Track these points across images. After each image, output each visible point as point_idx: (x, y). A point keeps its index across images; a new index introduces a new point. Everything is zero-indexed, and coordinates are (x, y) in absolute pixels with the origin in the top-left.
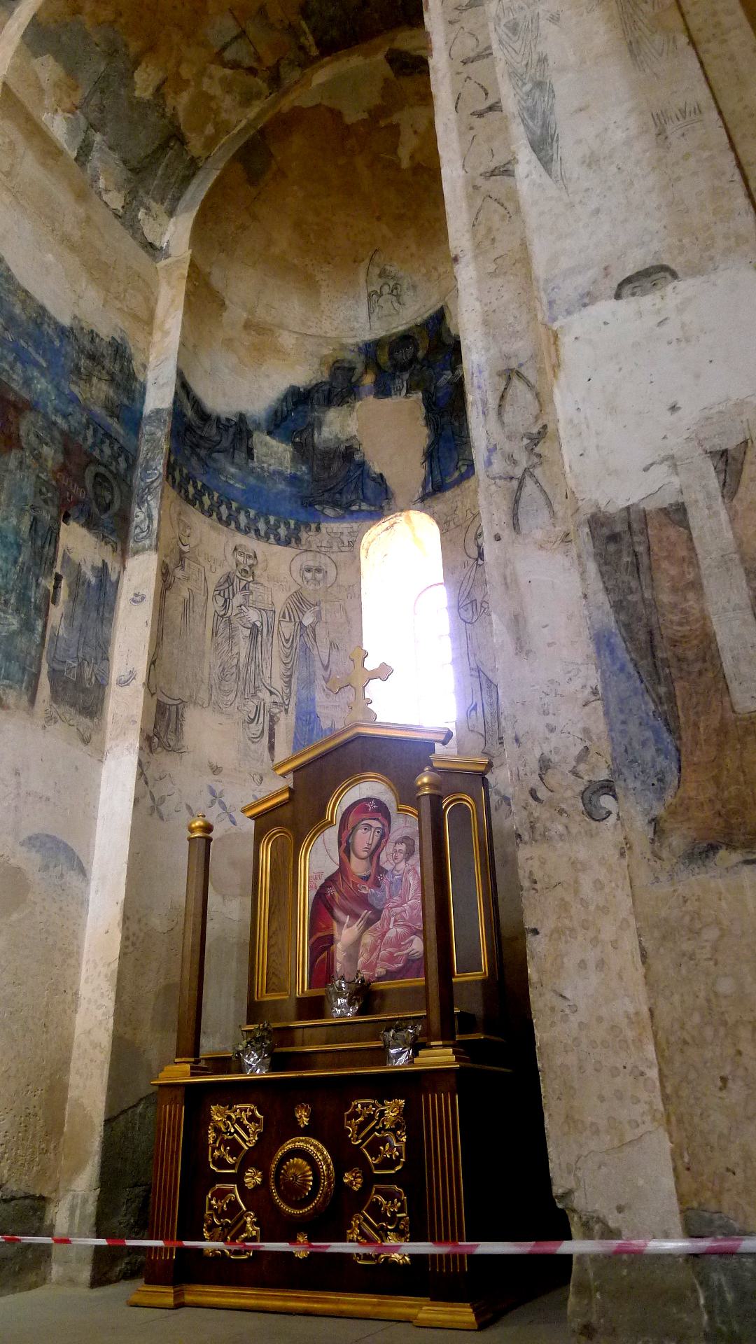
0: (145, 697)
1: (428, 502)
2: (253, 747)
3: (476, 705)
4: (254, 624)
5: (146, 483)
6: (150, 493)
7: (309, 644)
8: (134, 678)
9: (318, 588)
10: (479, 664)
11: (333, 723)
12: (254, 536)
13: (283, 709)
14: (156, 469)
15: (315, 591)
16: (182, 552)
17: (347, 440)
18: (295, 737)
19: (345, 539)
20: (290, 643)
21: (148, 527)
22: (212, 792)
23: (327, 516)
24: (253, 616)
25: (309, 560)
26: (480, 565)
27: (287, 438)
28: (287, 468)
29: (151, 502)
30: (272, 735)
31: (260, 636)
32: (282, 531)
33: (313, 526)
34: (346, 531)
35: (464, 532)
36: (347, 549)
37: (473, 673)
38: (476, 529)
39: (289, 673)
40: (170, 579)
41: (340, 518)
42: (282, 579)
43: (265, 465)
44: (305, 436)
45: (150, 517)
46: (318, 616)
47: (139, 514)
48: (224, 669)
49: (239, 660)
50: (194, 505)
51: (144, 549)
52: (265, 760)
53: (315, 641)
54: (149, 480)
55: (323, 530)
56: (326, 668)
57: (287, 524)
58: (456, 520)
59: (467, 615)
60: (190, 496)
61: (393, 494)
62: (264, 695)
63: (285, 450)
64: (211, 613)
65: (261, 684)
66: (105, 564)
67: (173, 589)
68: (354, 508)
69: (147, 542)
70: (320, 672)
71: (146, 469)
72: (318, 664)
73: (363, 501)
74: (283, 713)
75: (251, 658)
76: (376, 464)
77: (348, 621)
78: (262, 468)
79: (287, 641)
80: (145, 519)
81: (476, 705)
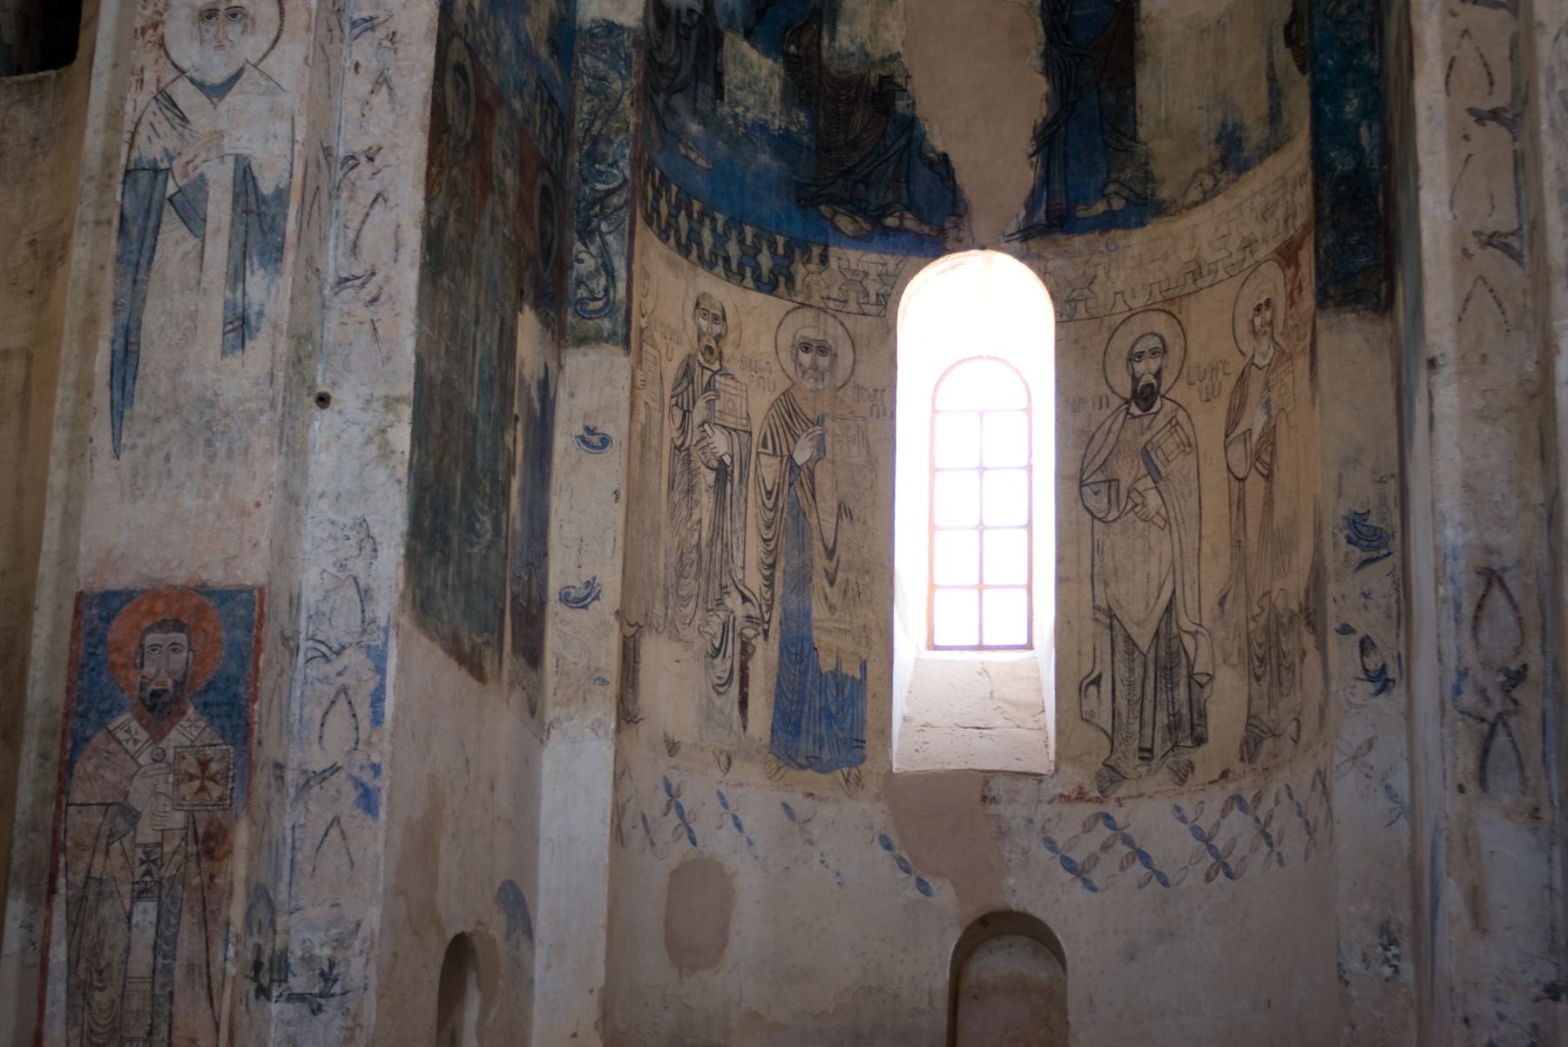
1: (1034, 245)
2: (718, 702)
3: (1100, 676)
4: (721, 461)
5: (593, 190)
7: (803, 502)
8: (597, 598)
9: (820, 386)
10: (1114, 606)
11: (839, 663)
12: (723, 274)
13: (760, 629)
14: (614, 164)
15: (816, 392)
17: (883, 61)
18: (779, 685)
19: (873, 287)
20: (773, 500)
21: (606, 291)
22: (668, 787)
23: (837, 229)
24: (720, 443)
25: (804, 325)
26: (1134, 417)
27: (773, 48)
28: (774, 114)
29: (610, 238)
30: (744, 682)
31: (729, 484)
32: (765, 261)
33: (816, 251)
34: (873, 271)
35: (1106, 335)
36: (873, 310)
37: (1098, 615)
38: (1132, 339)
39: (770, 561)
41: (861, 240)
42: (763, 364)
43: (740, 110)
44: (805, 40)
46: (821, 448)
47: (584, 256)
48: (682, 554)
49: (700, 535)
52: (735, 727)
53: (813, 496)
54: (600, 187)
55: (833, 263)
56: (831, 553)
57: (773, 245)
58: (1091, 303)
59: (1099, 504)
61: (966, 208)
62: (733, 602)
63: (772, 74)
64: (667, 440)
65: (729, 582)
68: (891, 221)
70: (820, 563)
72: (817, 544)
73: (908, 209)
74: (760, 638)
75: (717, 529)
76: (936, 128)
77: (872, 462)
78: (735, 117)
79: (769, 493)
81: (1100, 676)
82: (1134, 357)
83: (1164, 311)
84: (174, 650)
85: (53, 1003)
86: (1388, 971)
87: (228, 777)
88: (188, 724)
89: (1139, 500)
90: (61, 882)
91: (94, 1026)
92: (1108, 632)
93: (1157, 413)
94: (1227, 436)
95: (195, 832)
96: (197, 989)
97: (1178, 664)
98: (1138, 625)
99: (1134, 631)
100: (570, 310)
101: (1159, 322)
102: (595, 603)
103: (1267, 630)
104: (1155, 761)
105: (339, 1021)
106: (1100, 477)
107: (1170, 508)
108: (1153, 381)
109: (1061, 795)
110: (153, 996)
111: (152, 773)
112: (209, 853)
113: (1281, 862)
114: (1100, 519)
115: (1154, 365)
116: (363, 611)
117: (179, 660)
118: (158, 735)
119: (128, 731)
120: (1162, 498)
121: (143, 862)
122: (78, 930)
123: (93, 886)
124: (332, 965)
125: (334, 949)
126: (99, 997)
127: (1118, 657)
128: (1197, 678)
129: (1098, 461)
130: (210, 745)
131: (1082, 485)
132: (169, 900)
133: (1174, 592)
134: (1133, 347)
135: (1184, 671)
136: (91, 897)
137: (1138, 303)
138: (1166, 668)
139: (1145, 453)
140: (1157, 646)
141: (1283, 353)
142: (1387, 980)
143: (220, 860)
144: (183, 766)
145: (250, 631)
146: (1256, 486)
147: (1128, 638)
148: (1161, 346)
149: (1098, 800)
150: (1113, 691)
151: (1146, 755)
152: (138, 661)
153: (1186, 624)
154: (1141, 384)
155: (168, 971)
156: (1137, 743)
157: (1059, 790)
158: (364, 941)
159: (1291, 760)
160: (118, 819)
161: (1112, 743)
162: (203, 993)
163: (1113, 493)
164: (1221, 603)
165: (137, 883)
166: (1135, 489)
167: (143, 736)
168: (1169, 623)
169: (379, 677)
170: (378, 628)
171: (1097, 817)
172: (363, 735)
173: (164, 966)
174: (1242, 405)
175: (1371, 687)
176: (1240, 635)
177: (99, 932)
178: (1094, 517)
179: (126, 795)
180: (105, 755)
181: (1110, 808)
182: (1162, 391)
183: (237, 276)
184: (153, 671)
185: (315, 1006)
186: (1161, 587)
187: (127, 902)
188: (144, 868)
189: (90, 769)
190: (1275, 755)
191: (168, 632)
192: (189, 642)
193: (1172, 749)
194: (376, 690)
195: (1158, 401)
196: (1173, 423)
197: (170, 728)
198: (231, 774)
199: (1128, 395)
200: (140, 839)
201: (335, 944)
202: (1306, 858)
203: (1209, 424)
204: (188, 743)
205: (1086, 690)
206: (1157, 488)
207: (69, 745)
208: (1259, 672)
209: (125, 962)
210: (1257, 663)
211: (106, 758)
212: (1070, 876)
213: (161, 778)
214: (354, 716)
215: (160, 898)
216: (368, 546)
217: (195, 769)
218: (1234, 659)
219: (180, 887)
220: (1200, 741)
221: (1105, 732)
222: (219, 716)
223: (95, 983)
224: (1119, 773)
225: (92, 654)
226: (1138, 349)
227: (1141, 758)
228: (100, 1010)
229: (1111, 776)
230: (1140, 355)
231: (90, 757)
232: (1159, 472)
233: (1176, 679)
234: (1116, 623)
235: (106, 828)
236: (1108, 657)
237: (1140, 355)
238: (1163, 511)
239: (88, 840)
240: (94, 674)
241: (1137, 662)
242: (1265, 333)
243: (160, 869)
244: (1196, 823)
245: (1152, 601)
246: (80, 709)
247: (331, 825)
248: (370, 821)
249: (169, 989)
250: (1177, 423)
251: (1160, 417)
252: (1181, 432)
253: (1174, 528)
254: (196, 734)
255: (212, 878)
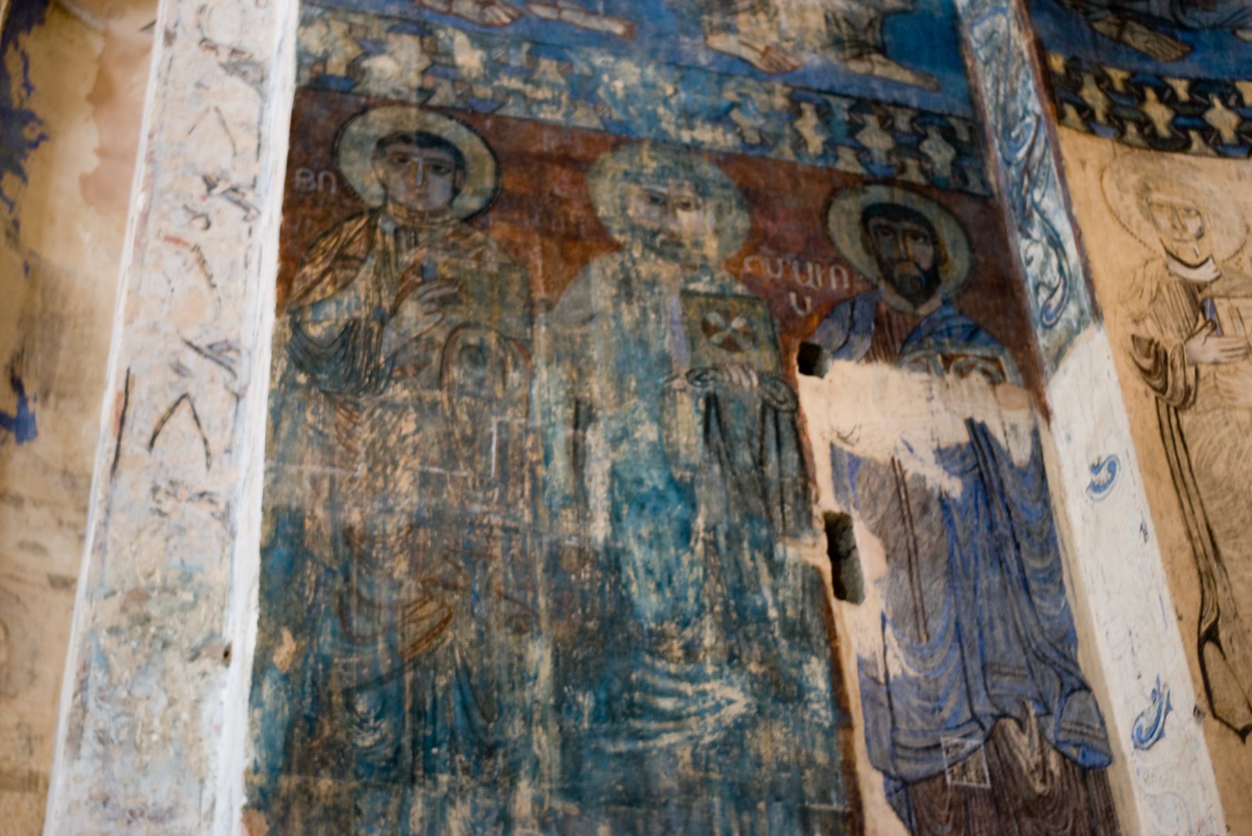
0: (1214, 755)
6: (1034, 183)
8: (1169, 708)
16: (1194, 291)
21: (1061, 269)
40: (1179, 377)
45: (1055, 242)
50: (1185, 147)
51: (1072, 333)
60: (1163, 131)
66: (977, 430)
67: (1203, 401)
69: (1072, 310)
71: (1008, 129)
80: (1047, 255)
100: (1039, 331)
102: (1171, 715)
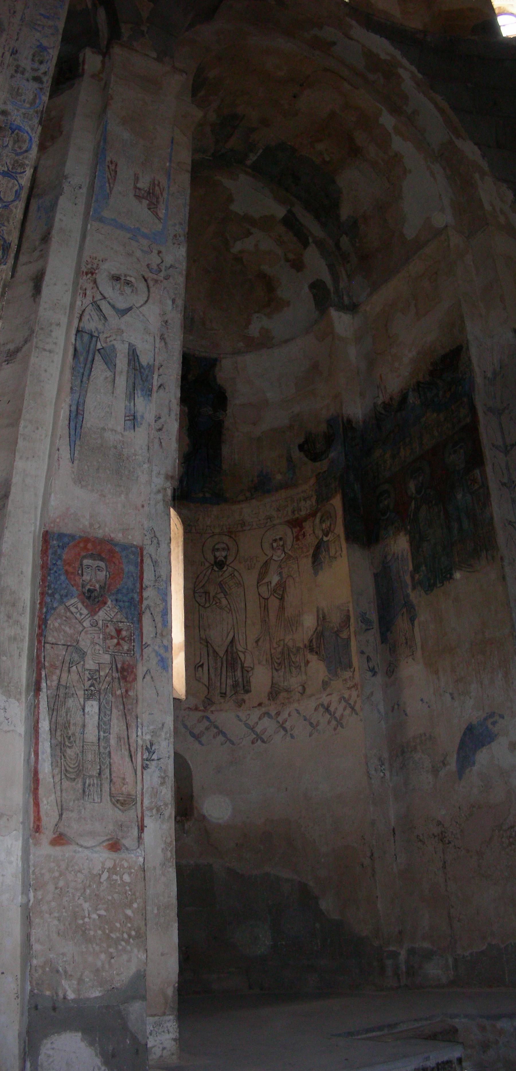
3: (203, 664)
26: (215, 571)
37: (202, 641)
81: (203, 664)
82: (214, 550)
83: (228, 536)
84: (99, 570)
85: (43, 753)
86: (382, 774)
87: (131, 640)
88: (108, 609)
89: (218, 601)
90: (44, 685)
91: (68, 768)
92: (206, 648)
93: (225, 571)
94: (258, 583)
95: (117, 666)
96: (123, 751)
97: (237, 663)
98: (219, 647)
99: (217, 649)
101: (225, 539)
103: (282, 653)
104: (227, 698)
105: (157, 773)
106: (202, 590)
107: (232, 605)
108: (223, 559)
109: (189, 708)
110: (100, 753)
111: (89, 632)
112: (125, 678)
113: (292, 736)
114: (202, 606)
115: (224, 554)
116: (155, 571)
117: (102, 575)
118: (93, 612)
119: (77, 608)
120: (228, 602)
121: (89, 680)
122: (55, 713)
123: (62, 690)
124: (152, 744)
125: (152, 736)
126: (69, 751)
127: (210, 658)
128: (245, 668)
129: (202, 584)
130: (121, 622)
131: (194, 592)
132: (104, 701)
133: (234, 636)
134: (214, 546)
135: (240, 666)
136: (62, 695)
137: (217, 531)
138: (231, 664)
139: (220, 585)
140: (227, 655)
141: (291, 556)
142: (382, 778)
143: (131, 682)
144: (108, 630)
145: (137, 567)
146: (274, 603)
147: (214, 651)
148: (227, 548)
149: (204, 711)
150: (209, 670)
151: (223, 695)
152: (80, 572)
153: (240, 648)
154: (218, 560)
155: (107, 740)
156: (219, 691)
157: (187, 706)
158: (166, 733)
159: (299, 700)
160: (74, 655)
161: (209, 689)
162: (127, 753)
163: (207, 597)
164: (257, 642)
165: (87, 690)
166: (216, 597)
167: (85, 611)
168: (232, 646)
169: (164, 604)
170: (162, 580)
171: (203, 717)
172: (159, 631)
173: (104, 737)
174: (266, 573)
175: (370, 674)
176: (267, 654)
177: (67, 715)
178: (199, 605)
179: (78, 642)
180: (64, 618)
181: (208, 714)
182: (228, 563)
183: (131, 396)
184: (88, 578)
185: (144, 765)
186: (228, 635)
187: (82, 700)
188: (90, 682)
189: (57, 625)
190: (288, 699)
191: (94, 560)
192: (106, 567)
193: (235, 694)
194: (163, 610)
195: (226, 566)
196: (232, 576)
197: (99, 610)
198: (132, 638)
199: (212, 562)
200: (87, 667)
201: (152, 734)
202: (310, 735)
203: (250, 579)
204: (109, 619)
205: (198, 668)
206: (226, 598)
207: (45, 610)
208: (277, 668)
209: (83, 733)
210: (276, 665)
211: (65, 621)
212: (193, 739)
213: (96, 635)
214: (154, 620)
215: (99, 700)
216: (155, 541)
217: (114, 633)
218: (264, 663)
219: (110, 695)
220: (247, 691)
221: (206, 685)
222: (124, 607)
223: (67, 743)
224: (212, 702)
225: (54, 564)
226: (217, 547)
227: (221, 696)
228: (71, 759)
229: (209, 702)
230: (218, 550)
231: (56, 619)
232: (226, 592)
233: (236, 668)
234: (209, 645)
235: (67, 658)
236: (206, 657)
237: (218, 550)
238: (228, 606)
239: (58, 664)
240: (57, 575)
241: (219, 660)
242: (279, 549)
243: (99, 684)
244: (247, 722)
245: (224, 639)
246: (50, 592)
247: (146, 673)
248: (165, 674)
249: (108, 750)
250: (234, 575)
251: (226, 572)
252: (236, 579)
253: (234, 612)
254: (113, 615)
255: (127, 691)
